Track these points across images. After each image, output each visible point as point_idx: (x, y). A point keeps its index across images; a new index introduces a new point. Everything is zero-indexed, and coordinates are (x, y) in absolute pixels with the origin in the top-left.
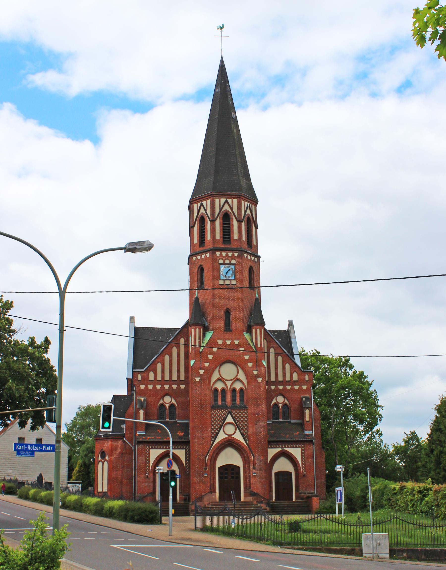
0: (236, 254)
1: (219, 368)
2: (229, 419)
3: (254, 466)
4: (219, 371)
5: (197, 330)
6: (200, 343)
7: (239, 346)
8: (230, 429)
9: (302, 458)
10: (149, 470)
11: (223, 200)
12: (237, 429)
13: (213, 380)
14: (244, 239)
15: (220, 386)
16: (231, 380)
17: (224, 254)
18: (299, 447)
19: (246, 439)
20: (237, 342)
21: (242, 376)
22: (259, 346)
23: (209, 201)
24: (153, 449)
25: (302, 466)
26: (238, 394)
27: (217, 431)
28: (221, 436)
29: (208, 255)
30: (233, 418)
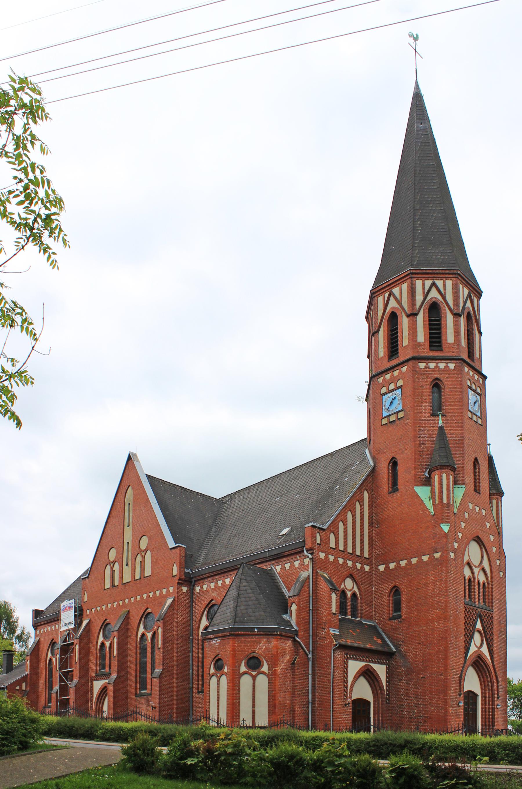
11: (428, 283)
23: (405, 286)
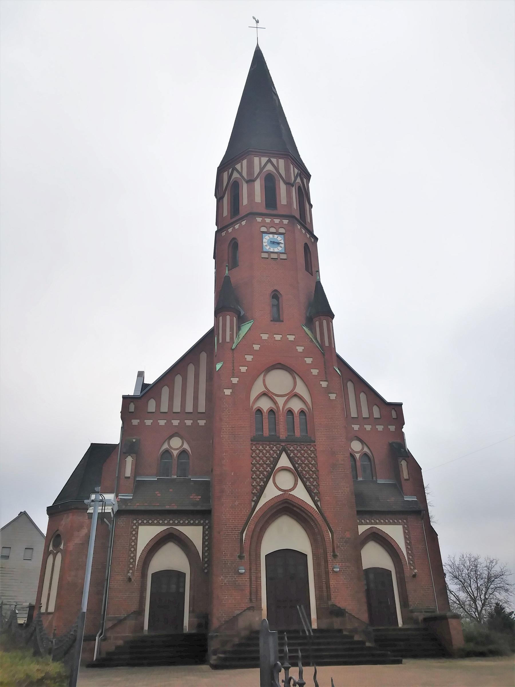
0: (286, 222)
1: (265, 376)
2: (284, 461)
3: (334, 551)
4: (264, 381)
5: (228, 318)
6: (232, 338)
7: (295, 343)
8: (286, 480)
10: (134, 566)
11: (264, 160)
12: (300, 481)
13: (254, 394)
14: (295, 206)
15: (265, 405)
17: (268, 220)
18: (399, 524)
19: (316, 498)
20: (291, 338)
21: (301, 389)
22: (327, 344)
23: (245, 162)
24: (145, 524)
27: (262, 483)
28: (271, 493)
29: (244, 223)
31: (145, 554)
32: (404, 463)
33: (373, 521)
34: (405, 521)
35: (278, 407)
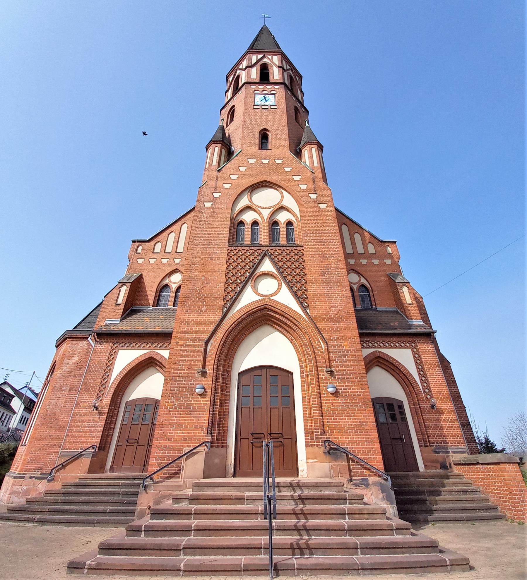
2: (267, 266)
5: (217, 149)
9: (418, 368)
12: (284, 285)
16: (270, 208)
18: (406, 347)
21: (289, 201)
25: (423, 386)
26: (282, 229)
28: (248, 298)
30: (275, 264)
31: (119, 379)
32: (405, 289)
33: (376, 345)
34: (413, 345)
35: (262, 218)
